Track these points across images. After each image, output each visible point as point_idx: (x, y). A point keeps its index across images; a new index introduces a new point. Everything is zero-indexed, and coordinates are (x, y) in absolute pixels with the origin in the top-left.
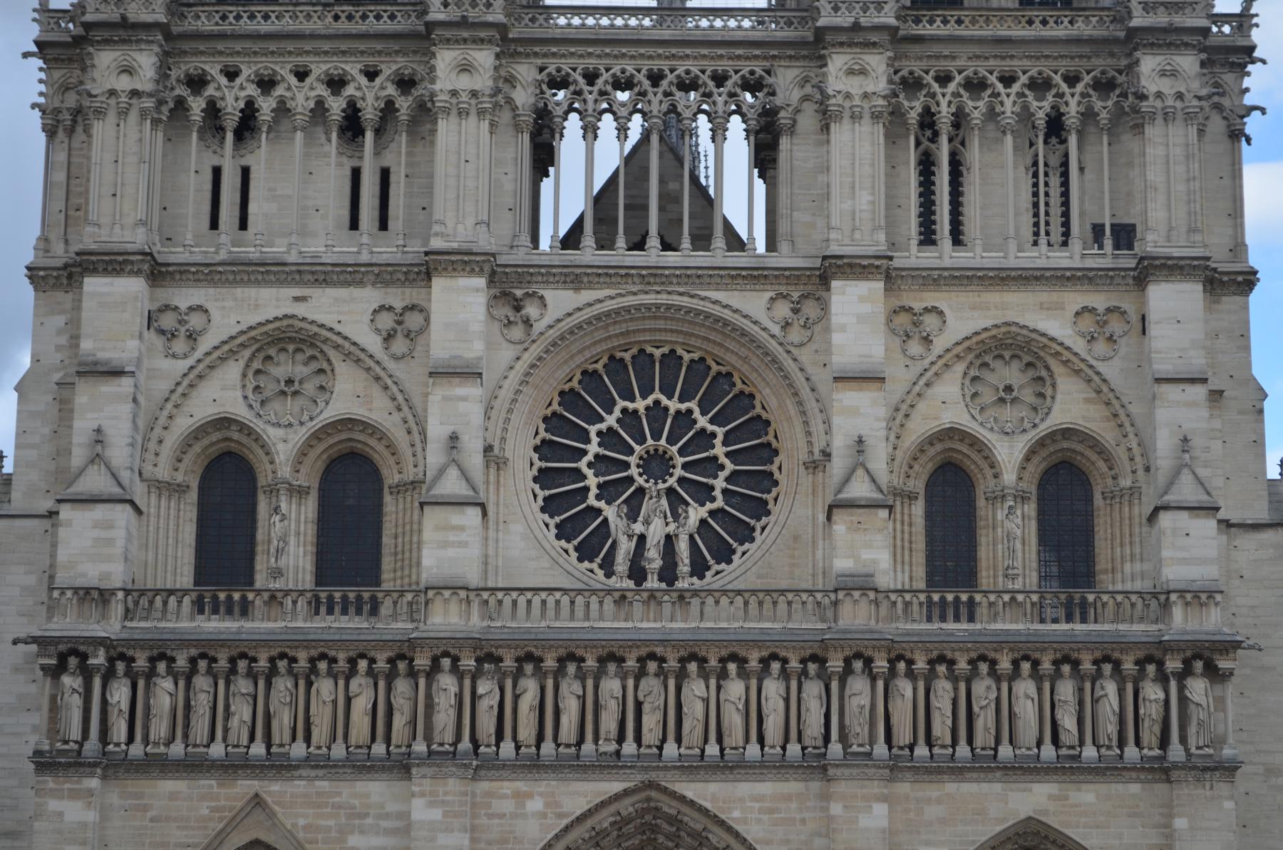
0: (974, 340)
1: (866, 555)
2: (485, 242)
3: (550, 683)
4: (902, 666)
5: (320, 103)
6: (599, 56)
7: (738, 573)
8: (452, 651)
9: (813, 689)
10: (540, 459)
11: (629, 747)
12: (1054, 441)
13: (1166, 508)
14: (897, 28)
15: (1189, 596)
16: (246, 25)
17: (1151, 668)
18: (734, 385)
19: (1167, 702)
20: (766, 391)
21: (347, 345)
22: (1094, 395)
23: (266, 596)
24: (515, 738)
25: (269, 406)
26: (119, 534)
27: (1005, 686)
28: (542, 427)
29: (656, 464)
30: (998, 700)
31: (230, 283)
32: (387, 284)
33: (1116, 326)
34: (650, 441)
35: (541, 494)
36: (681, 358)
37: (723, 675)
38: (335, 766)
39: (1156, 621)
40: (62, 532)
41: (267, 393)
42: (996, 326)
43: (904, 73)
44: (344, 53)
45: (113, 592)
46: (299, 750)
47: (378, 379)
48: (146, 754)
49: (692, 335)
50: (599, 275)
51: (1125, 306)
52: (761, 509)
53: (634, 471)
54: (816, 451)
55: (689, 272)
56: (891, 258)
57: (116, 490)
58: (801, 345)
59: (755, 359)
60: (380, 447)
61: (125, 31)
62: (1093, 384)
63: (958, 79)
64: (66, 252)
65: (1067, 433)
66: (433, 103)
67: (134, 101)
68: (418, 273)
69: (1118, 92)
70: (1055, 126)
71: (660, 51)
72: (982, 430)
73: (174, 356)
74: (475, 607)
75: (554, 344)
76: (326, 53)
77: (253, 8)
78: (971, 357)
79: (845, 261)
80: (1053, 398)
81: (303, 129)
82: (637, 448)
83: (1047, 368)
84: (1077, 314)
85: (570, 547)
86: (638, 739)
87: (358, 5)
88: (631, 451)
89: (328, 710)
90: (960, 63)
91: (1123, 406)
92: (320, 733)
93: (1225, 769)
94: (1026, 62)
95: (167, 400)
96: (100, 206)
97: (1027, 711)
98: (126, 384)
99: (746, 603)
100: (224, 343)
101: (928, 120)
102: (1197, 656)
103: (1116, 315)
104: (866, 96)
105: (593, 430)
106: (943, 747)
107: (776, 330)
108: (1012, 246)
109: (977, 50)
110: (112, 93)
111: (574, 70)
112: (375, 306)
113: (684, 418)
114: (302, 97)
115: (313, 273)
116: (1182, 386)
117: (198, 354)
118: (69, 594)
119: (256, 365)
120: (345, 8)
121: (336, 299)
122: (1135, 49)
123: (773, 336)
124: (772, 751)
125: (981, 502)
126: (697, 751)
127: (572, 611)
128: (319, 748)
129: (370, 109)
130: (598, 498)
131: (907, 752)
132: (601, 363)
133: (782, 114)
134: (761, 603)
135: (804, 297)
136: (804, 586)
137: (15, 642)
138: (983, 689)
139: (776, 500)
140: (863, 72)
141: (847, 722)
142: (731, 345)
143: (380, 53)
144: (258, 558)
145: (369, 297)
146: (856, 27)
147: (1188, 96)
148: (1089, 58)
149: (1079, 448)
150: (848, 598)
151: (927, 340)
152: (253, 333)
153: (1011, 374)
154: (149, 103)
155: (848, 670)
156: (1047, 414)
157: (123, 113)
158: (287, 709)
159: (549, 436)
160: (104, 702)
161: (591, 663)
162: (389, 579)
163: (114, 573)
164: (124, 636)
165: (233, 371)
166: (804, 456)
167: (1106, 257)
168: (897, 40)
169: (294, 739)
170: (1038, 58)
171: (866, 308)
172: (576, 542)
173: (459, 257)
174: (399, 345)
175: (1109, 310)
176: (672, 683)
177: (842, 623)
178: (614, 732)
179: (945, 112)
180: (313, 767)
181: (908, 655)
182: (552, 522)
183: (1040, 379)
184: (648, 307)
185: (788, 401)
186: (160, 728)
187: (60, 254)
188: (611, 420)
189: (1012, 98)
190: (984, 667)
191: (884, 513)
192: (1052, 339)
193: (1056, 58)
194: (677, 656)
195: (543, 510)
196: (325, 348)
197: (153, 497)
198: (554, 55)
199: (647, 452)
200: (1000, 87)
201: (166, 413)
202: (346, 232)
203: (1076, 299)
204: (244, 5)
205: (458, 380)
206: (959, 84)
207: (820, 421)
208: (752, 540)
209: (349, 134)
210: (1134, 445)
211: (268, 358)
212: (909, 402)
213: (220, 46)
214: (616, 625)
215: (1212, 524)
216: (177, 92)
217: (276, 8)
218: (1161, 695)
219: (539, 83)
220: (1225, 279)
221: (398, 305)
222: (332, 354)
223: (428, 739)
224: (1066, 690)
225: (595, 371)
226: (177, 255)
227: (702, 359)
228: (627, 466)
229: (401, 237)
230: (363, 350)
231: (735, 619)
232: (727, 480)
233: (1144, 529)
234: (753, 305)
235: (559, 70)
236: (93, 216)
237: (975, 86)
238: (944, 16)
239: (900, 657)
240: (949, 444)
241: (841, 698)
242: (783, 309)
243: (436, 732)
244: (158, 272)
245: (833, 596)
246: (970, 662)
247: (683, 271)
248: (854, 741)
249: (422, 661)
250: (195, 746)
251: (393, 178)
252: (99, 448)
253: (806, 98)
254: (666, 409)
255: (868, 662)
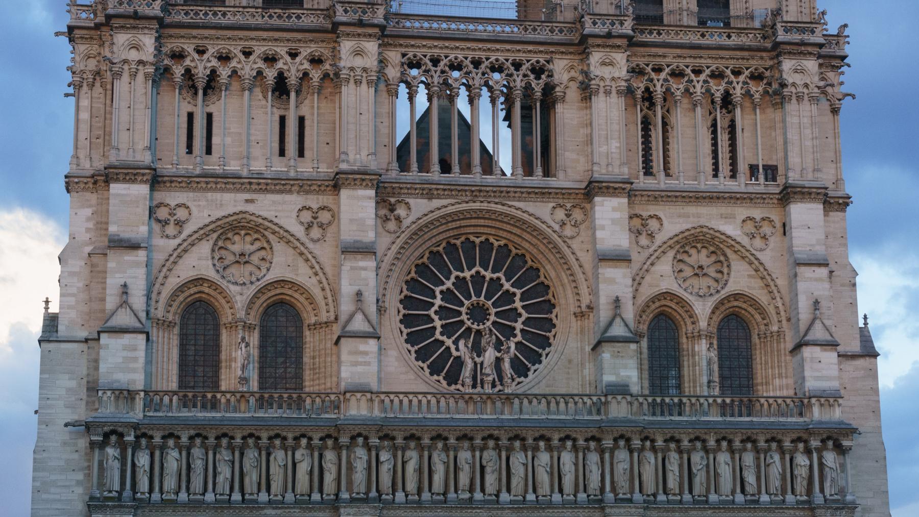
0: (680, 236)
1: (623, 373)
2: (373, 166)
3: (426, 453)
4: (648, 443)
5: (260, 73)
6: (441, 48)
7: (533, 383)
8: (364, 433)
9: (593, 458)
10: (404, 308)
11: (478, 496)
12: (729, 301)
13: (807, 344)
14: (634, 37)
15: (822, 400)
16: (211, 19)
17: (801, 446)
18: (526, 262)
19: (811, 467)
20: (548, 267)
21: (282, 232)
22: (754, 273)
23: (238, 395)
24: (404, 489)
25: (228, 271)
26: (141, 354)
27: (711, 456)
28: (405, 287)
29: (479, 313)
30: (708, 466)
31: (204, 189)
32: (307, 192)
33: (766, 229)
34: (474, 298)
35: (405, 331)
36: (492, 244)
37: (536, 449)
38: (289, 508)
39: (801, 414)
40: (102, 353)
41: (227, 262)
42: (694, 228)
43: (634, 65)
44: (276, 40)
45: (137, 392)
46: (263, 497)
47: (301, 254)
48: (162, 500)
49: (501, 229)
50: (445, 190)
51: (773, 217)
52: (545, 343)
53: (464, 317)
54: (583, 306)
55: (502, 189)
56: (632, 183)
57: (138, 325)
58: (572, 238)
59: (541, 245)
60: (302, 299)
61: (136, 20)
62: (753, 266)
63: (667, 70)
64: (91, 166)
65: (737, 296)
66: (337, 75)
67: (140, 67)
68: (327, 186)
69: (765, 82)
70: (727, 101)
71: (480, 46)
72: (685, 294)
73: (167, 237)
74: (376, 404)
75: (415, 234)
76: (264, 40)
77: (216, 9)
78: (678, 246)
79: (604, 184)
80: (728, 274)
81: (250, 90)
82: (466, 302)
83: (725, 255)
84: (744, 221)
85: (425, 366)
86: (483, 490)
87: (285, 9)
88: (462, 304)
89: (282, 471)
90: (668, 60)
91: (773, 280)
92: (276, 487)
93: (848, 508)
94: (709, 61)
95: (164, 266)
96: (122, 139)
97: (725, 472)
98: (141, 255)
99: (548, 403)
100: (202, 229)
101: (646, 95)
102: (829, 438)
103: (766, 222)
104: (613, 79)
105: (438, 290)
106: (674, 495)
107: (557, 227)
108: (702, 178)
109: (678, 51)
110: (125, 61)
111: (425, 56)
112: (300, 207)
113: (496, 283)
114: (248, 68)
115: (259, 184)
116: (813, 268)
117: (183, 236)
118: (109, 393)
119: (220, 243)
120: (276, 11)
121: (274, 202)
122: (778, 56)
123: (554, 232)
124: (568, 498)
125: (684, 340)
126: (521, 498)
127: (438, 407)
128: (276, 495)
129: (293, 78)
130: (442, 334)
131: (652, 498)
132: (442, 246)
133: (558, 89)
134: (558, 403)
135: (574, 206)
136: (576, 392)
137: (66, 425)
138: (697, 458)
139: (554, 336)
140: (611, 64)
141: (616, 479)
142: (527, 236)
143: (300, 41)
144: (223, 371)
145: (295, 201)
146: (609, 35)
147: (812, 86)
148: (748, 59)
149: (744, 306)
150: (614, 400)
151: (651, 236)
152: (219, 223)
153: (701, 257)
154: (151, 70)
155: (616, 447)
156: (725, 284)
157: (133, 75)
158: (255, 470)
159: (409, 294)
160: (134, 465)
161: (452, 441)
162: (309, 385)
163: (137, 380)
164: (146, 422)
165: (205, 248)
166: (573, 308)
167: (760, 185)
168: (632, 43)
169: (259, 490)
170: (716, 59)
171: (617, 215)
172: (428, 362)
173: (358, 176)
174: (316, 233)
175: (763, 219)
176: (504, 454)
177: (610, 416)
178: (467, 488)
179: (659, 90)
180: (274, 508)
181: (652, 437)
182: (413, 350)
183: (720, 261)
184: (475, 211)
185: (563, 274)
186: (170, 483)
187: (87, 167)
188: (449, 284)
189: (701, 83)
190: (699, 445)
191: (633, 346)
192: (729, 237)
193: (727, 59)
194: (507, 437)
195: (407, 341)
196: (266, 233)
197: (155, 330)
198: (413, 46)
199: (472, 305)
200: (693, 76)
201: (162, 274)
202: (276, 159)
203: (742, 212)
204: (210, 7)
205: (359, 256)
206: (668, 74)
207: (585, 287)
208: (540, 362)
209: (277, 93)
210: (780, 305)
211: (228, 239)
212: (641, 275)
213: (195, 32)
214: (467, 417)
215: (836, 354)
216: (166, 62)
217: (223, 9)
218: (808, 462)
219: (403, 64)
220: (832, 201)
221: (315, 206)
222: (271, 237)
223: (350, 489)
224: (749, 458)
225: (438, 252)
226: (166, 168)
227: (506, 245)
228: (460, 313)
229: (315, 162)
230: (292, 235)
231: (543, 414)
232: (523, 323)
233: (788, 358)
234: (543, 212)
235: (415, 56)
236: (115, 143)
237: (677, 74)
238: (659, 31)
239: (646, 438)
240: (663, 302)
241: (612, 464)
242: (560, 214)
243: (355, 485)
244: (156, 181)
245: (603, 399)
246: (690, 441)
247: (498, 189)
248: (621, 491)
249: (344, 440)
250: (195, 494)
251: (307, 123)
252: (125, 296)
253: (572, 79)
254: (484, 277)
255: (628, 440)
